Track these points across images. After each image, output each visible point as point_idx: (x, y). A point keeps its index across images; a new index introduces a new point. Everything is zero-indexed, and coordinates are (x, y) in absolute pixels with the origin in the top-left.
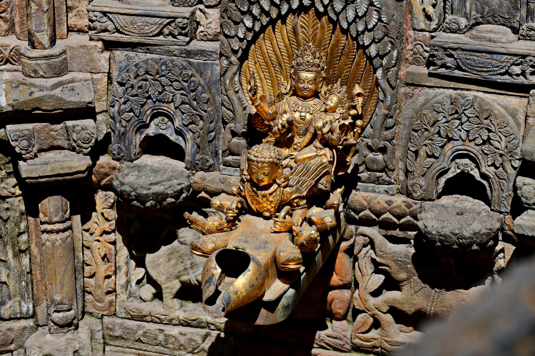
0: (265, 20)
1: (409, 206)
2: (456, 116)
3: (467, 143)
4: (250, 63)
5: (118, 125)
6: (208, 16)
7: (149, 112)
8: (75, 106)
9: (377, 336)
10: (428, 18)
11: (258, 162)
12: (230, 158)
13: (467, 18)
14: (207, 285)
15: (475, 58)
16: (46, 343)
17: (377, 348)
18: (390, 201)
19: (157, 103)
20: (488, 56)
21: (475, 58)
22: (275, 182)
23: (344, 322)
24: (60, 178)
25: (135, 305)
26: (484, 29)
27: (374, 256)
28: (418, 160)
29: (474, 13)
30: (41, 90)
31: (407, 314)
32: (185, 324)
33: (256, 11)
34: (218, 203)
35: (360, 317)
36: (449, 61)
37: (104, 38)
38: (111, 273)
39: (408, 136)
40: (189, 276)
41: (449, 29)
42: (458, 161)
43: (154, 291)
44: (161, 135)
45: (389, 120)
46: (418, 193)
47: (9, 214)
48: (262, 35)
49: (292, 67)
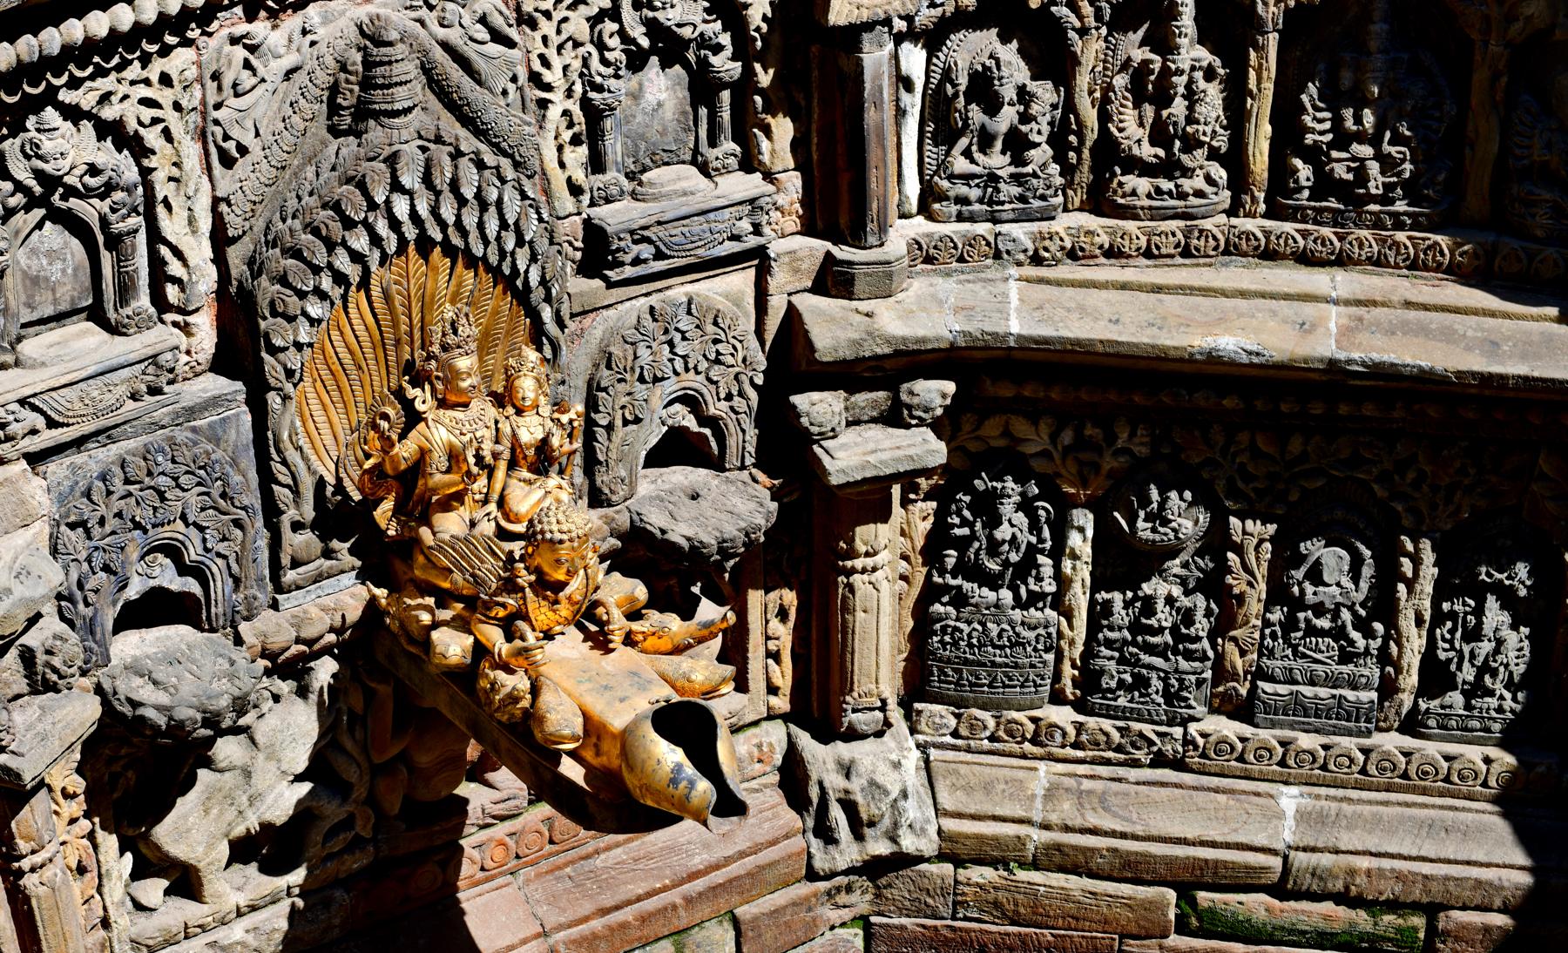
0: (340, 291)
3: (684, 376)
4: (307, 383)
5: (81, 606)
6: (194, 330)
10: (575, 190)
14: (683, 784)
15: (685, 230)
19: (150, 533)
20: (701, 218)
21: (685, 230)
26: (666, 178)
33: (326, 283)
34: (458, 651)
36: (646, 251)
37: (32, 449)
43: (165, 883)
44: (153, 589)
45: (561, 388)
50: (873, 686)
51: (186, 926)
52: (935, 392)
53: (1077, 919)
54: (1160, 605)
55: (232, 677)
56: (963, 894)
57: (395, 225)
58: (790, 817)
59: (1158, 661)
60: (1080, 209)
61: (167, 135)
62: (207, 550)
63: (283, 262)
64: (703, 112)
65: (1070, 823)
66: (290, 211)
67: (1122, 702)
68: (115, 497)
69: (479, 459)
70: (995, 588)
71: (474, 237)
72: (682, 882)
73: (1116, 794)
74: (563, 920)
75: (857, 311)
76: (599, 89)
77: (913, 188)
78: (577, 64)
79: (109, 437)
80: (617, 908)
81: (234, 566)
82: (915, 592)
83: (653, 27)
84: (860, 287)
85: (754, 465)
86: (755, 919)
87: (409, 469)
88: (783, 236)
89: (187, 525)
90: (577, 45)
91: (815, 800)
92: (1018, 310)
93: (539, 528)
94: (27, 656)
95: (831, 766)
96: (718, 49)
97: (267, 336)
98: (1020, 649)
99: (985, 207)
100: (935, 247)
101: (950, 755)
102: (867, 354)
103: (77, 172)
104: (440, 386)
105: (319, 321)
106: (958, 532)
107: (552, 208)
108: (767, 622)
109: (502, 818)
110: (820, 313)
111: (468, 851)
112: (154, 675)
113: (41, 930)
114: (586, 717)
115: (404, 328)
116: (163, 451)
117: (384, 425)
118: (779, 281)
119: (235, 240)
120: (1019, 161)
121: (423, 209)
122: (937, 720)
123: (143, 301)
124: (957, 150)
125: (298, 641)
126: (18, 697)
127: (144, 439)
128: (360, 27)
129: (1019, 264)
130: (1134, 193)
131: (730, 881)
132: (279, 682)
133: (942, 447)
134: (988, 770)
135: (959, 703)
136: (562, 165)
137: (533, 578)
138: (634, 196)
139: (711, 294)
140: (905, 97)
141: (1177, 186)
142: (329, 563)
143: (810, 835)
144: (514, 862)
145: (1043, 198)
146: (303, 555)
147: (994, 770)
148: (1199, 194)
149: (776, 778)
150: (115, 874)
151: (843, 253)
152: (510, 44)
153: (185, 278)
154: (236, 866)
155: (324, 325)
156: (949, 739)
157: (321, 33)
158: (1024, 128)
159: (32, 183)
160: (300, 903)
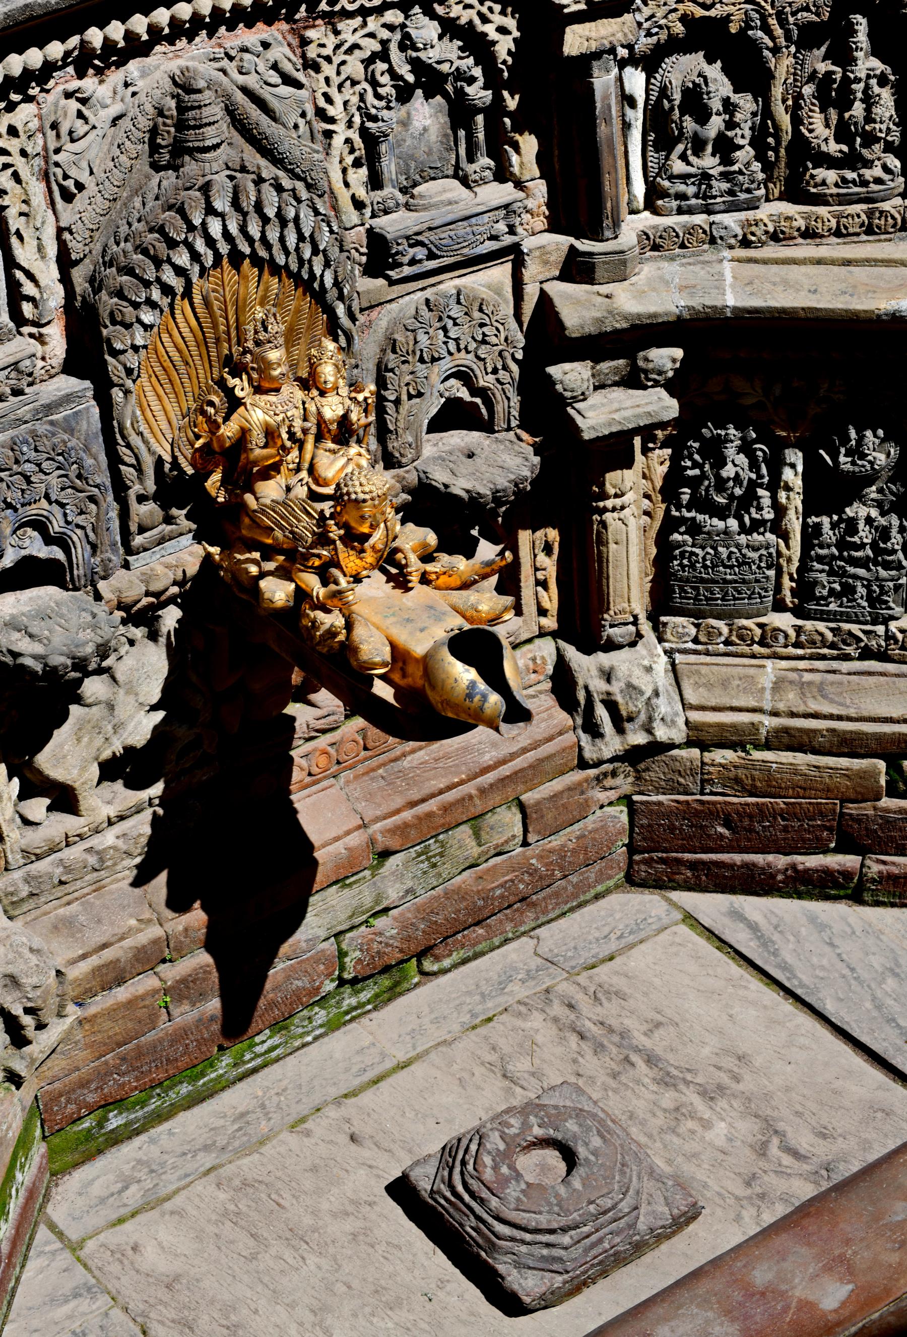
0: (165, 302)
3: (457, 355)
6: (47, 339)
10: (359, 205)
14: (478, 698)
20: (465, 223)
25: (35, 838)
33: (156, 294)
36: (421, 253)
43: (47, 801)
44: (25, 557)
45: (355, 371)
51: (67, 837)
52: (666, 357)
53: (805, 789)
54: (861, 526)
55: (95, 627)
56: (709, 773)
57: (210, 242)
58: (562, 717)
59: (861, 572)
60: (780, 199)
61: (16, 177)
62: (68, 523)
63: (119, 279)
64: (462, 133)
65: (794, 710)
66: (122, 236)
67: (833, 607)
69: (292, 435)
70: (723, 518)
72: (476, 776)
73: (832, 683)
74: (378, 813)
75: (599, 294)
76: (375, 119)
77: (639, 188)
78: (355, 100)
80: (423, 800)
82: (657, 524)
83: (417, 65)
84: (599, 274)
85: (519, 427)
86: (538, 803)
87: (232, 446)
88: (533, 234)
89: (50, 503)
90: (354, 83)
91: (582, 702)
92: (733, 286)
93: (345, 490)
95: (594, 672)
96: (471, 80)
97: (108, 341)
99: (700, 201)
101: (692, 658)
102: (609, 329)
104: (255, 376)
105: (151, 326)
106: (690, 473)
107: (340, 221)
109: (324, 731)
110: (567, 297)
111: (297, 760)
112: (30, 630)
114: (394, 647)
115: (222, 328)
116: (27, 442)
117: (211, 410)
118: (532, 271)
119: (77, 262)
120: (727, 161)
121: (233, 228)
124: (674, 156)
125: (148, 594)
127: (11, 433)
128: (173, 78)
129: (731, 247)
130: (824, 183)
131: (516, 773)
132: (133, 629)
133: (674, 403)
134: (724, 669)
135: (697, 615)
136: (347, 185)
137: (342, 532)
138: (408, 207)
140: (629, 112)
141: (859, 176)
142: (169, 528)
143: (580, 731)
144: (336, 767)
145: (748, 191)
146: (147, 522)
147: (729, 669)
148: (878, 181)
149: (548, 685)
151: (584, 245)
152: (299, 85)
153: (38, 296)
154: (106, 784)
155: (155, 329)
156: (690, 645)
157: (141, 85)
158: (729, 134)
160: (160, 811)
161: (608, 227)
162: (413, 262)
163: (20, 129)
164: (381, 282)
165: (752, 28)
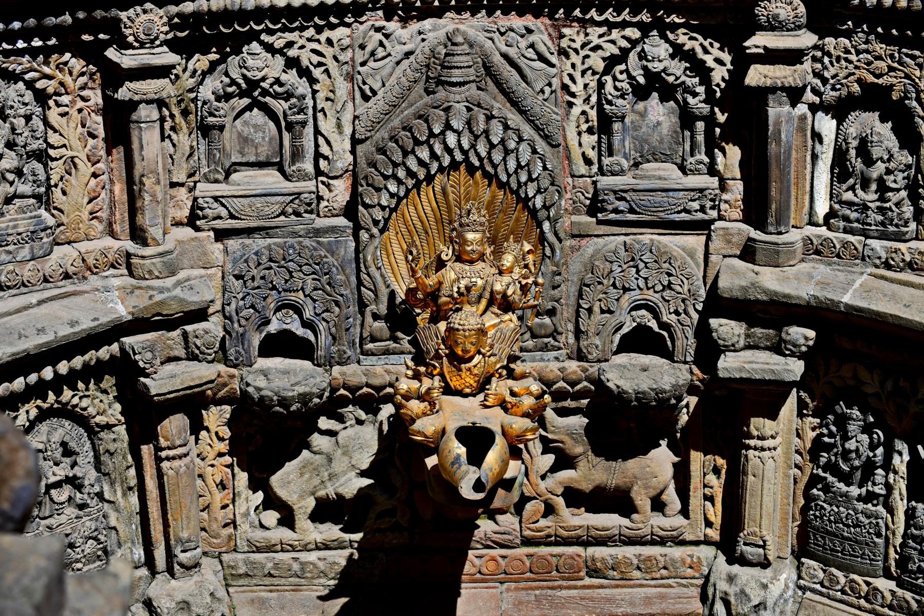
0: (410, 183)
1: (585, 370)
2: (631, 263)
3: (645, 291)
4: (391, 233)
5: (236, 325)
6: (333, 188)
7: (272, 305)
8: (197, 307)
9: (550, 524)
10: (588, 162)
11: (463, 330)
12: (370, 346)
13: (627, 159)
14: (457, 466)
15: (650, 198)
16: (174, 590)
17: (550, 536)
18: (564, 368)
19: (283, 294)
20: (664, 194)
21: (650, 198)
22: (479, 352)
23: (508, 514)
24: (188, 392)
25: (259, 534)
27: (544, 433)
28: (592, 317)
29: (632, 152)
30: (161, 292)
31: (585, 493)
32: (323, 547)
33: (401, 173)
34: (405, 387)
35: (529, 506)
36: (622, 205)
38: (228, 502)
39: (577, 294)
40: (327, 491)
41: (611, 172)
42: (634, 313)
43: (278, 516)
44: (285, 330)
45: (557, 278)
46: (595, 354)
47: (116, 445)
48: (405, 201)
49: (454, 229)
50: (757, 530)
61: (327, 71)
62: (315, 313)
68: (262, 267)
71: (500, 169)
76: (610, 103)
78: (593, 84)
79: (267, 234)
81: (333, 330)
82: (805, 479)
83: (647, 72)
84: (759, 257)
85: (694, 363)
88: (730, 221)
89: (305, 296)
91: (711, 597)
94: (185, 335)
95: (724, 576)
96: (695, 95)
97: (361, 195)
98: (858, 530)
100: (821, 244)
101: (818, 598)
102: (752, 298)
103: (268, 81)
104: (457, 247)
108: (705, 475)
109: (502, 546)
113: (167, 495)
120: (882, 199)
121: (466, 145)
122: (812, 571)
123: (309, 167)
125: (368, 385)
126: (177, 359)
129: (877, 267)
136: (580, 145)
137: (447, 351)
139: (672, 245)
142: (395, 345)
145: (897, 226)
150: (243, 496)
153: (331, 157)
156: (818, 587)
157: (430, 36)
158: (885, 177)
159: (241, 81)
161: (772, 224)
162: (616, 211)
163: (335, 41)
164: (594, 219)
165: (909, 99)
